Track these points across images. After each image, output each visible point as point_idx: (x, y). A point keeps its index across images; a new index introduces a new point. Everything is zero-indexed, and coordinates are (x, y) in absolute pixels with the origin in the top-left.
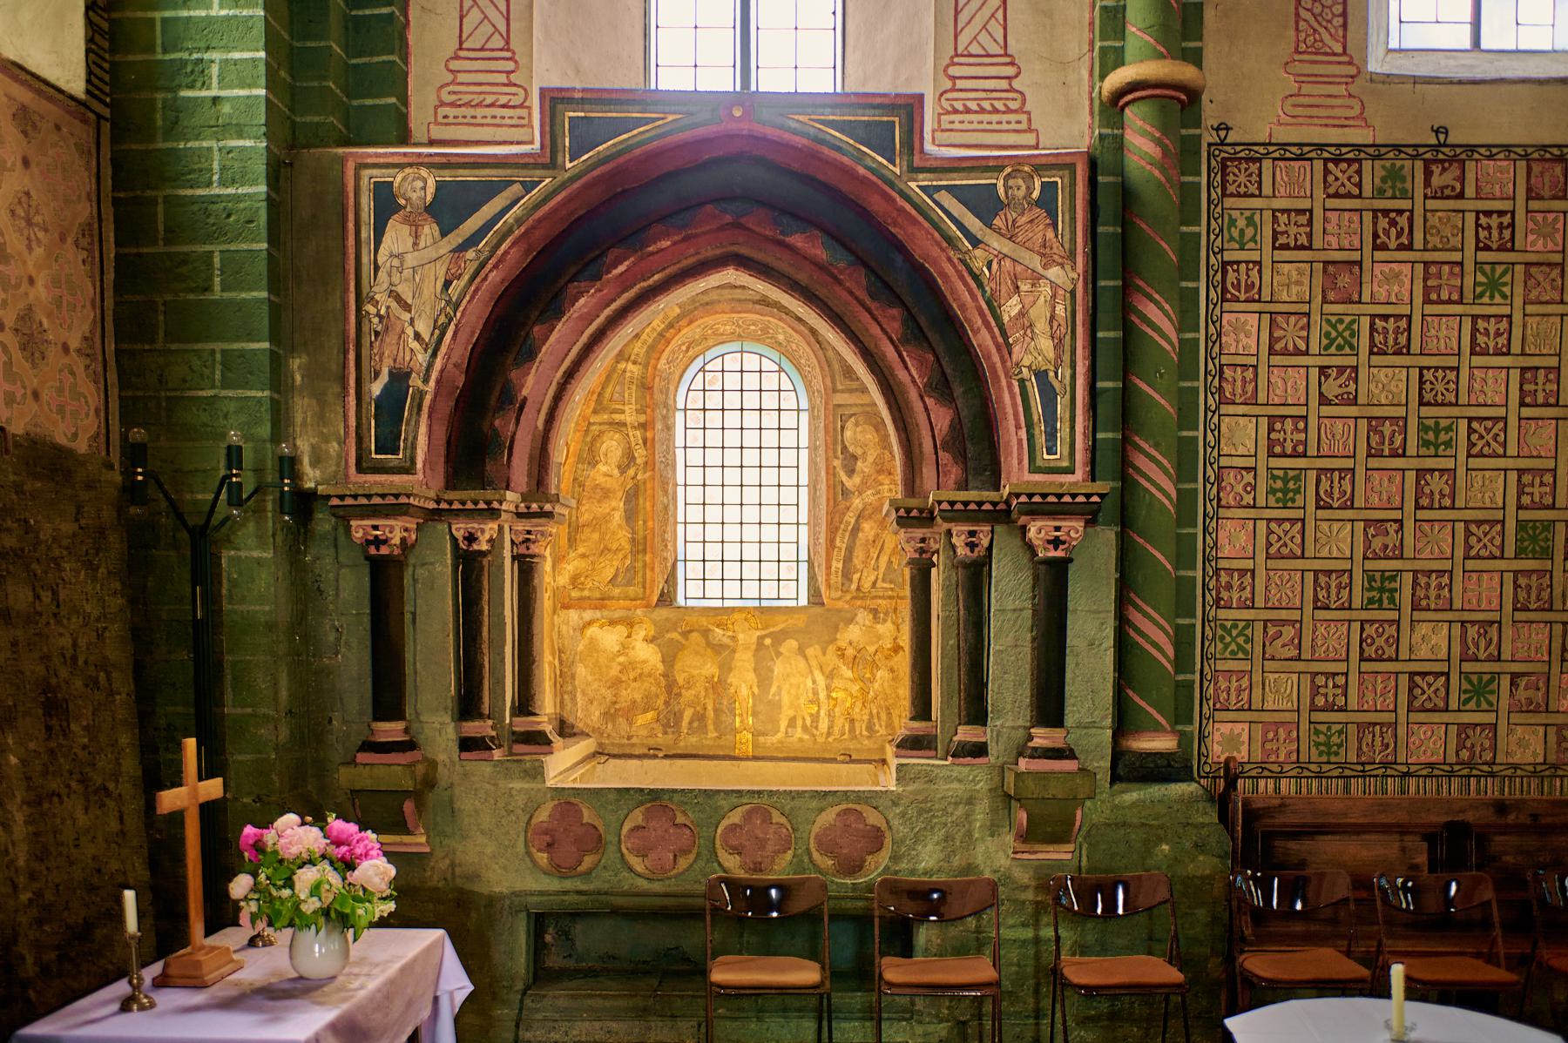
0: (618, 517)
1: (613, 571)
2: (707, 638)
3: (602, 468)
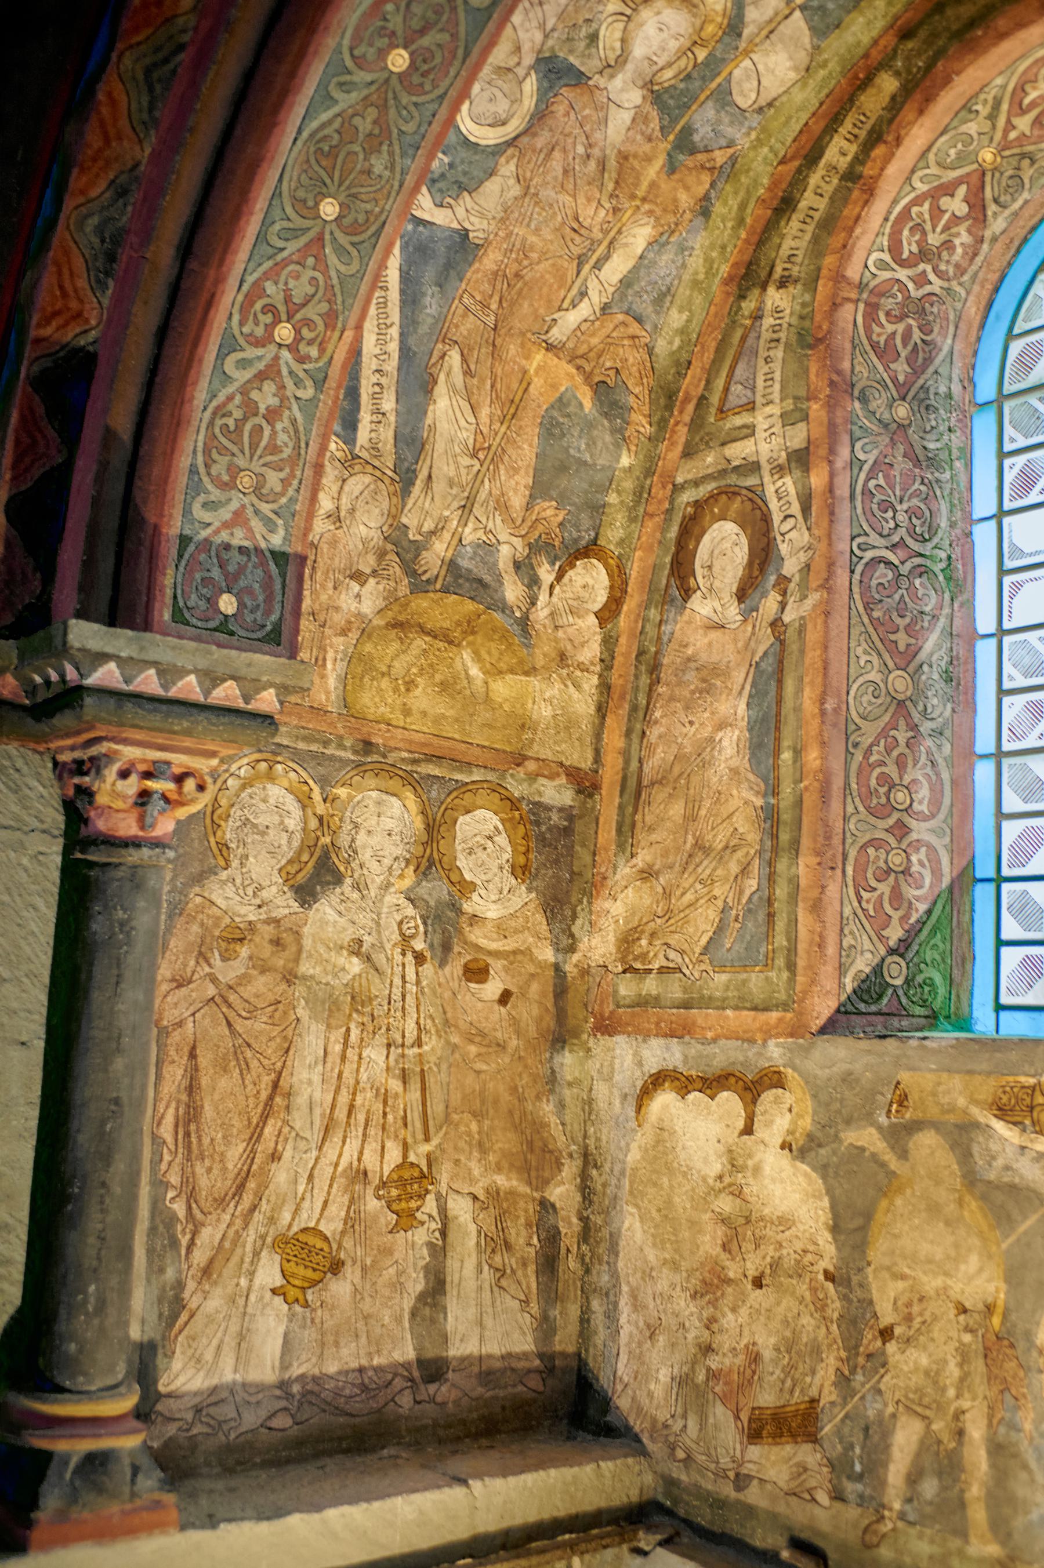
0: (731, 746)
1: (712, 914)
2: (965, 1156)
3: (701, 607)
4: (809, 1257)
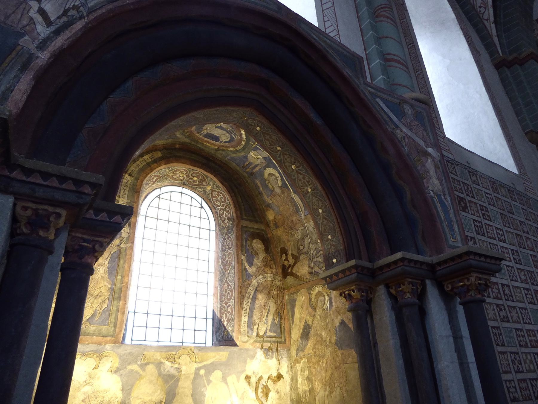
4: (113, 399)
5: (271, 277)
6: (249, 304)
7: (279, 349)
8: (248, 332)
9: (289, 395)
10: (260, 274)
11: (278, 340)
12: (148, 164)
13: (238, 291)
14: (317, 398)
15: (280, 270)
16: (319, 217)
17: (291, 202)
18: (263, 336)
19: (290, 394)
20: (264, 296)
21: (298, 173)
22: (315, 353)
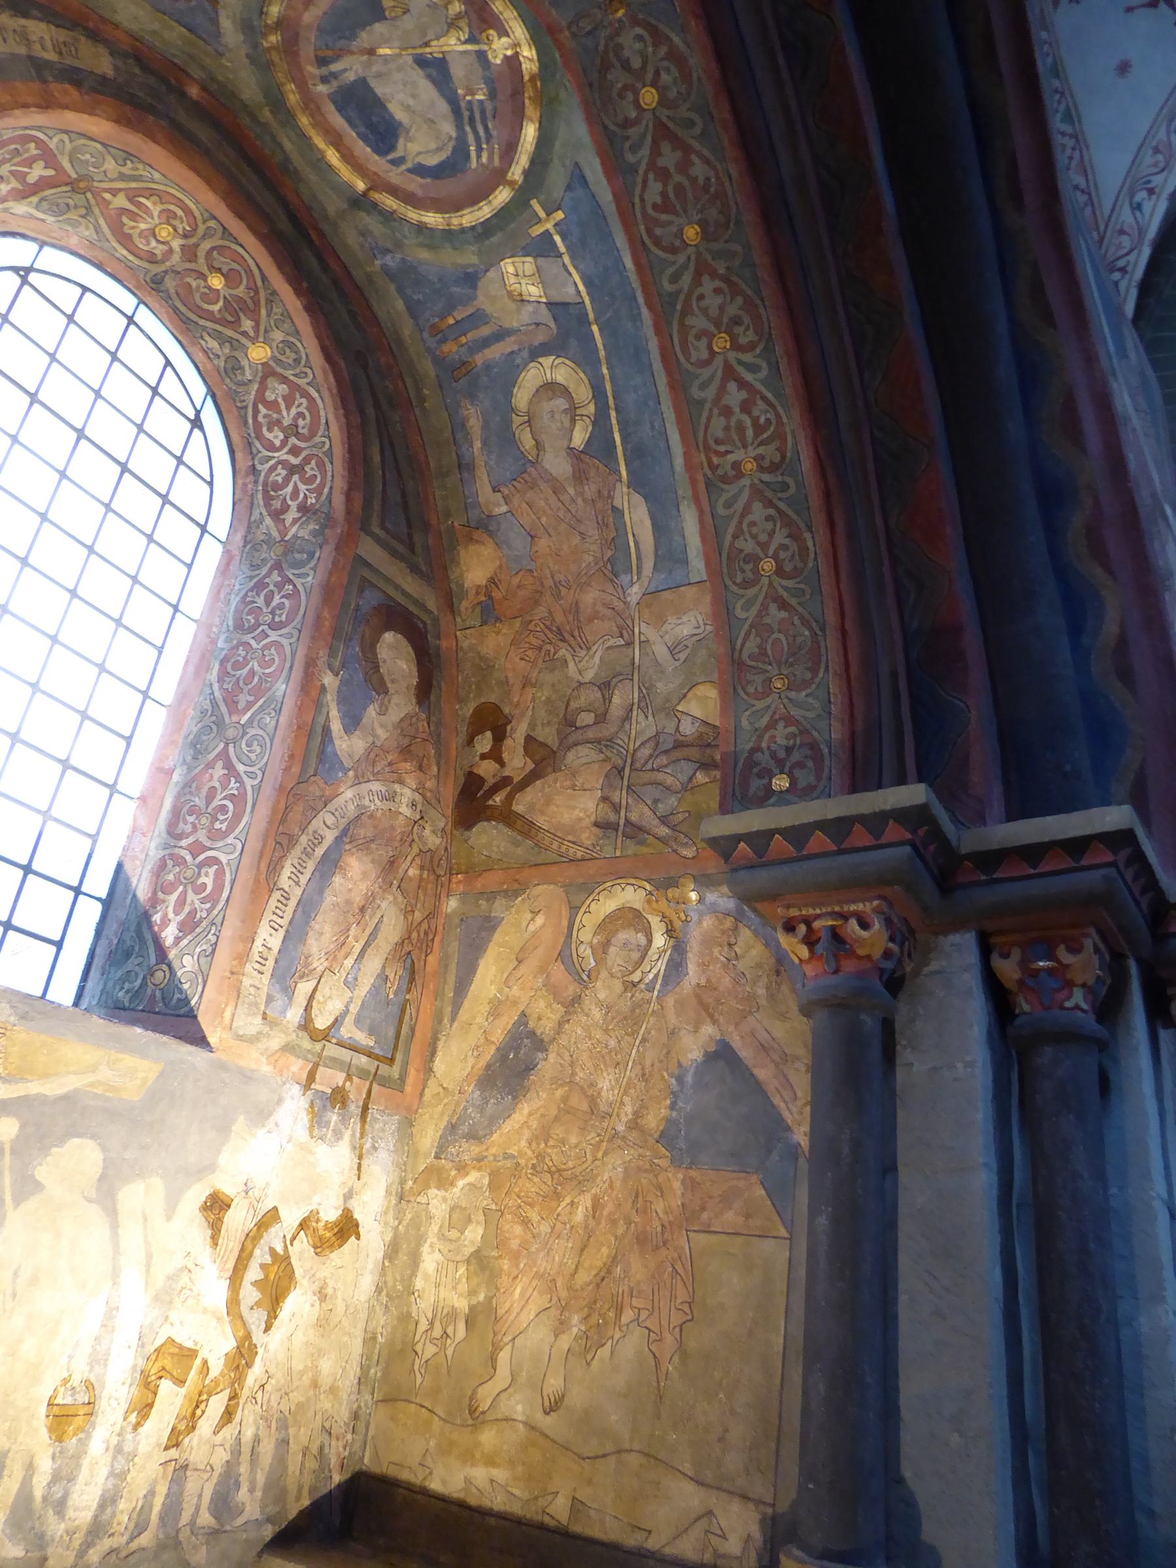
5: (414, 805)
6: (304, 879)
7: (373, 1110)
8: (270, 999)
9: (363, 1316)
10: (377, 776)
11: (372, 1075)
12: (39, 68)
13: (274, 810)
14: (504, 1357)
15: (450, 792)
16: (751, 592)
17: (602, 525)
18: (324, 1036)
19: (371, 1310)
20: (370, 866)
21: (729, 373)
22: (540, 1157)
